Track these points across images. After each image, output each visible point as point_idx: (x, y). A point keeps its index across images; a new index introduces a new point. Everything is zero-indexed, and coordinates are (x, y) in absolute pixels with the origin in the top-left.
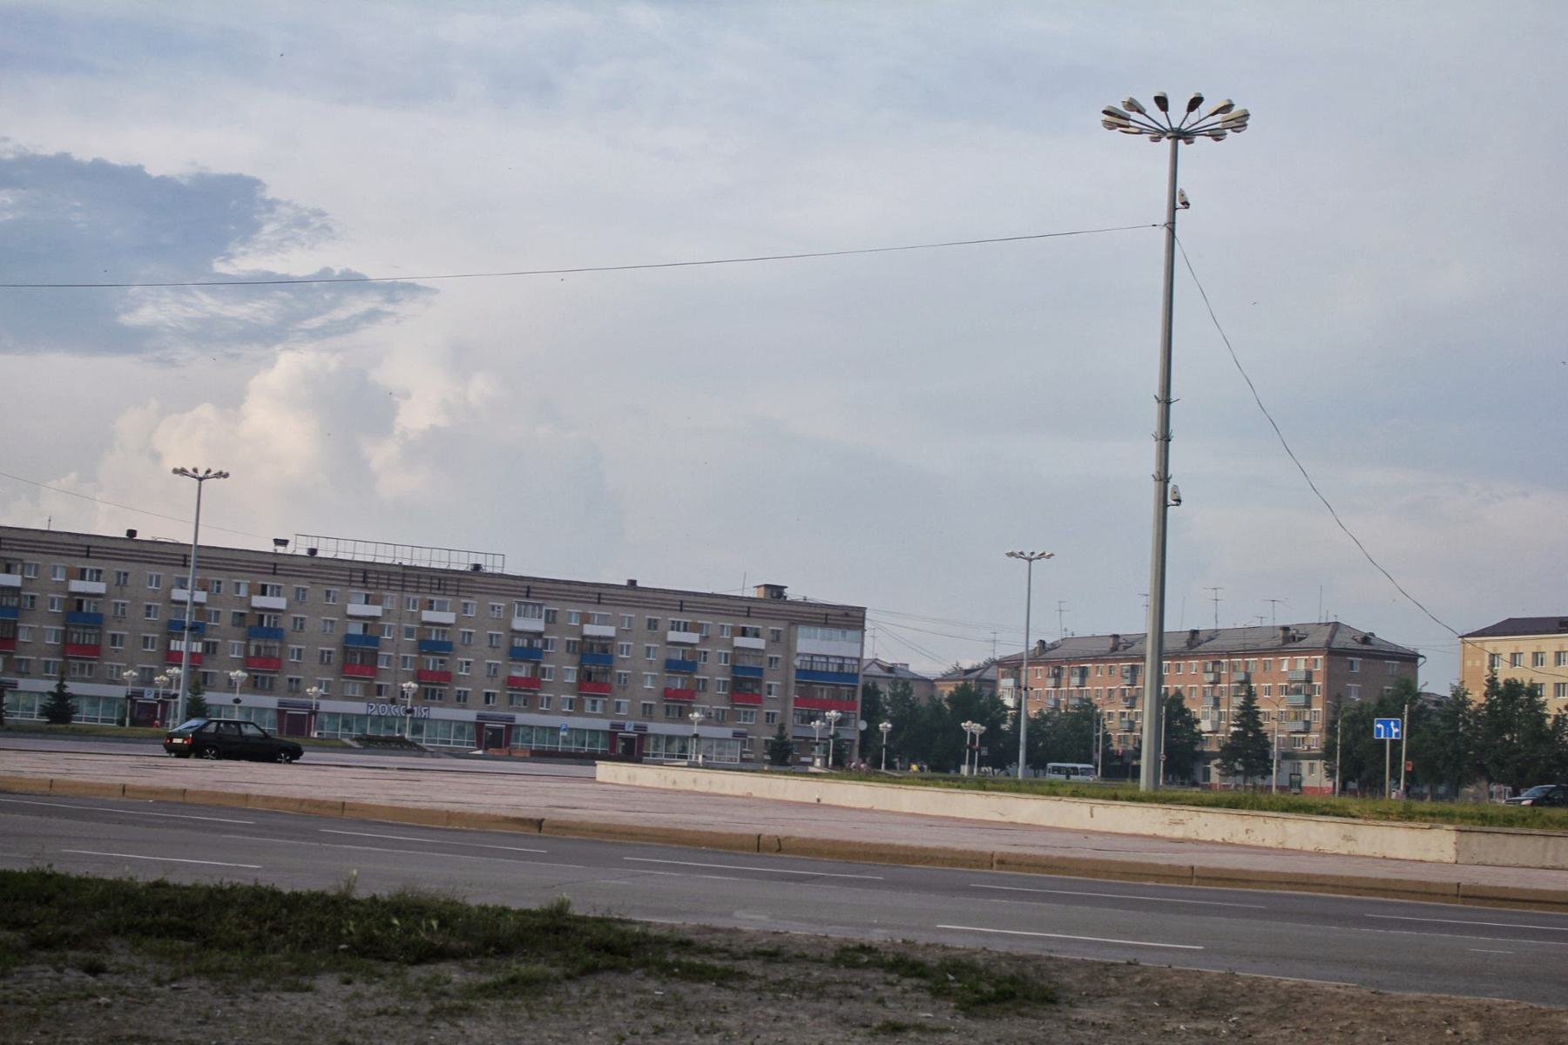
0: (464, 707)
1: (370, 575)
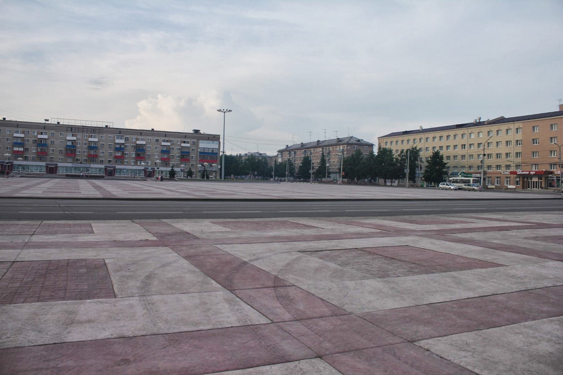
0: (102, 164)
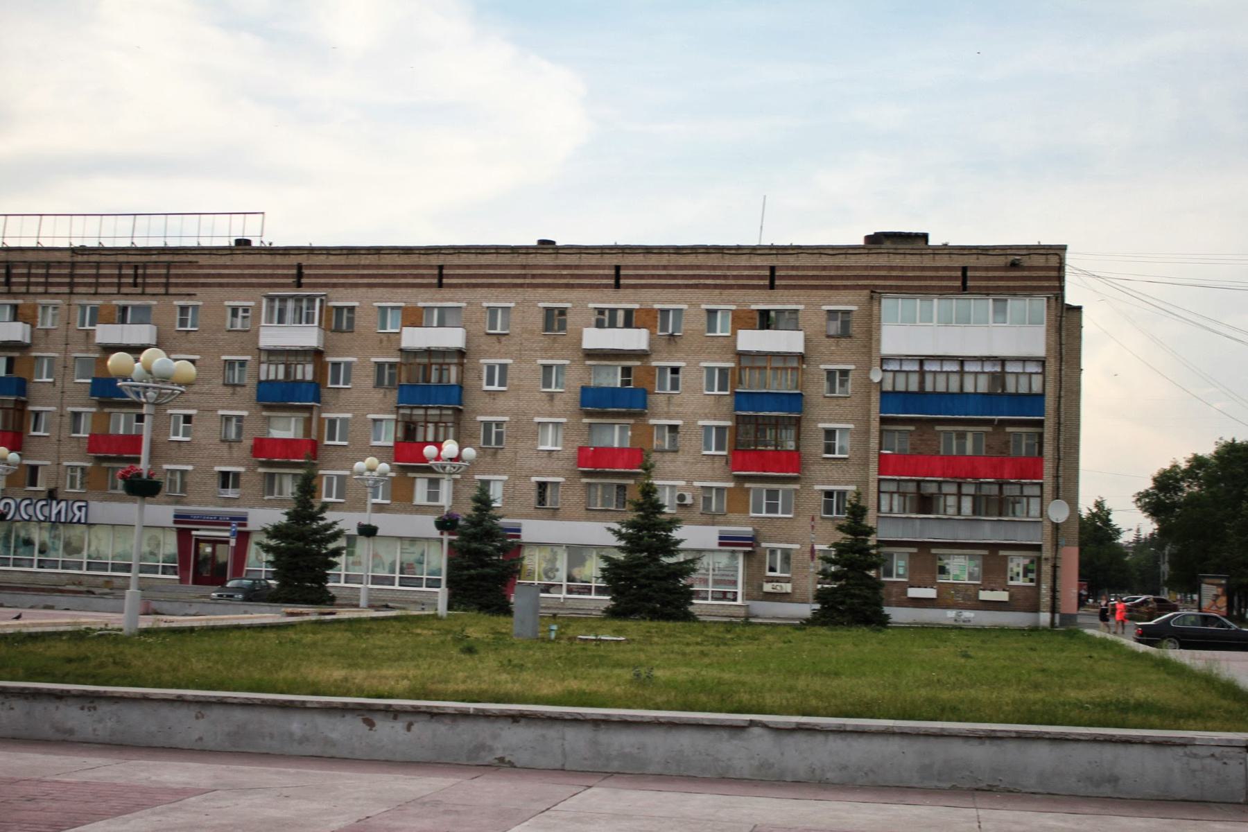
1: (14, 271)
